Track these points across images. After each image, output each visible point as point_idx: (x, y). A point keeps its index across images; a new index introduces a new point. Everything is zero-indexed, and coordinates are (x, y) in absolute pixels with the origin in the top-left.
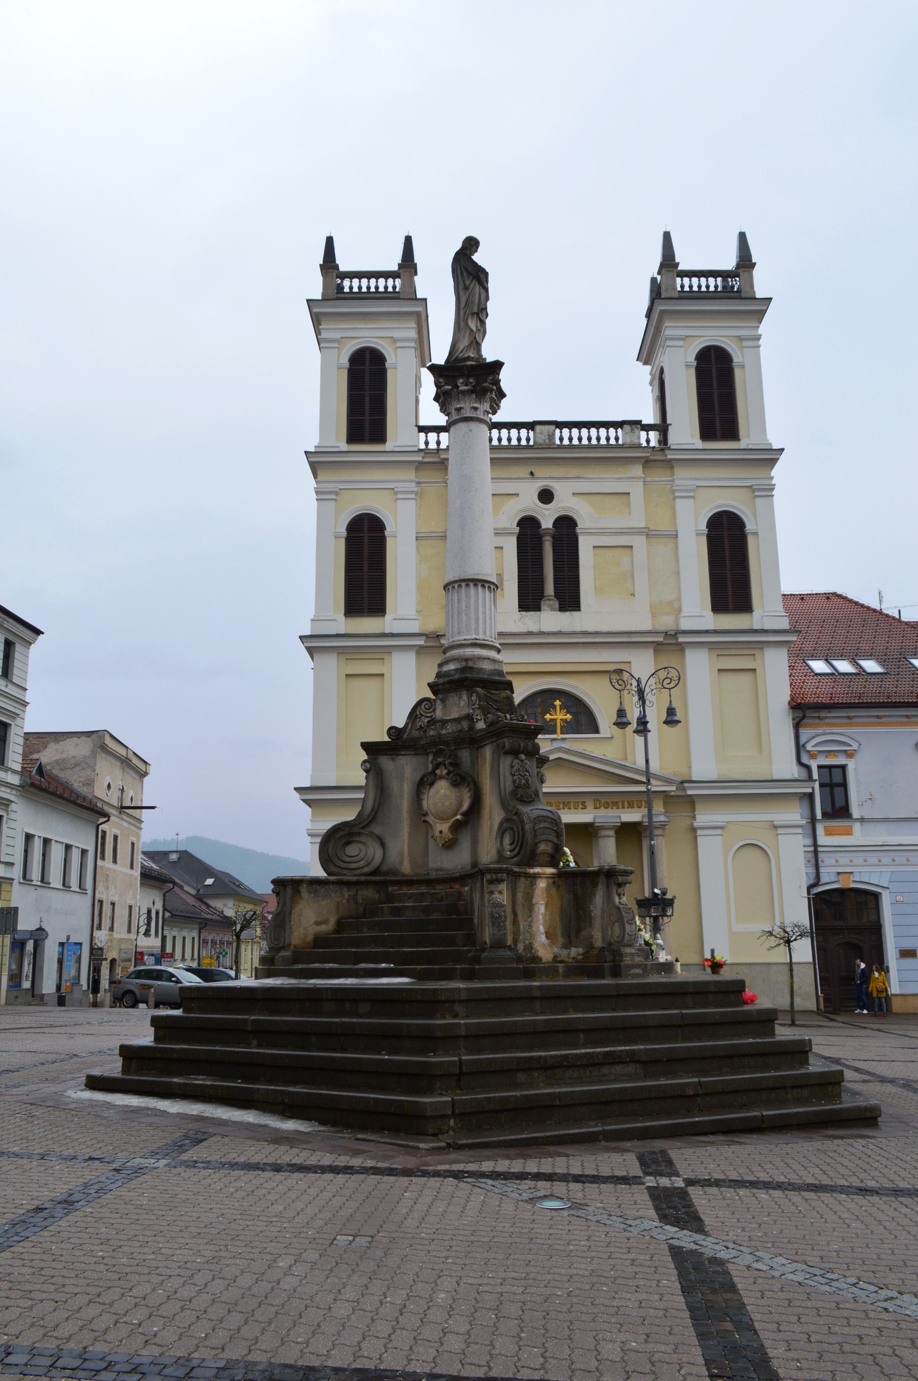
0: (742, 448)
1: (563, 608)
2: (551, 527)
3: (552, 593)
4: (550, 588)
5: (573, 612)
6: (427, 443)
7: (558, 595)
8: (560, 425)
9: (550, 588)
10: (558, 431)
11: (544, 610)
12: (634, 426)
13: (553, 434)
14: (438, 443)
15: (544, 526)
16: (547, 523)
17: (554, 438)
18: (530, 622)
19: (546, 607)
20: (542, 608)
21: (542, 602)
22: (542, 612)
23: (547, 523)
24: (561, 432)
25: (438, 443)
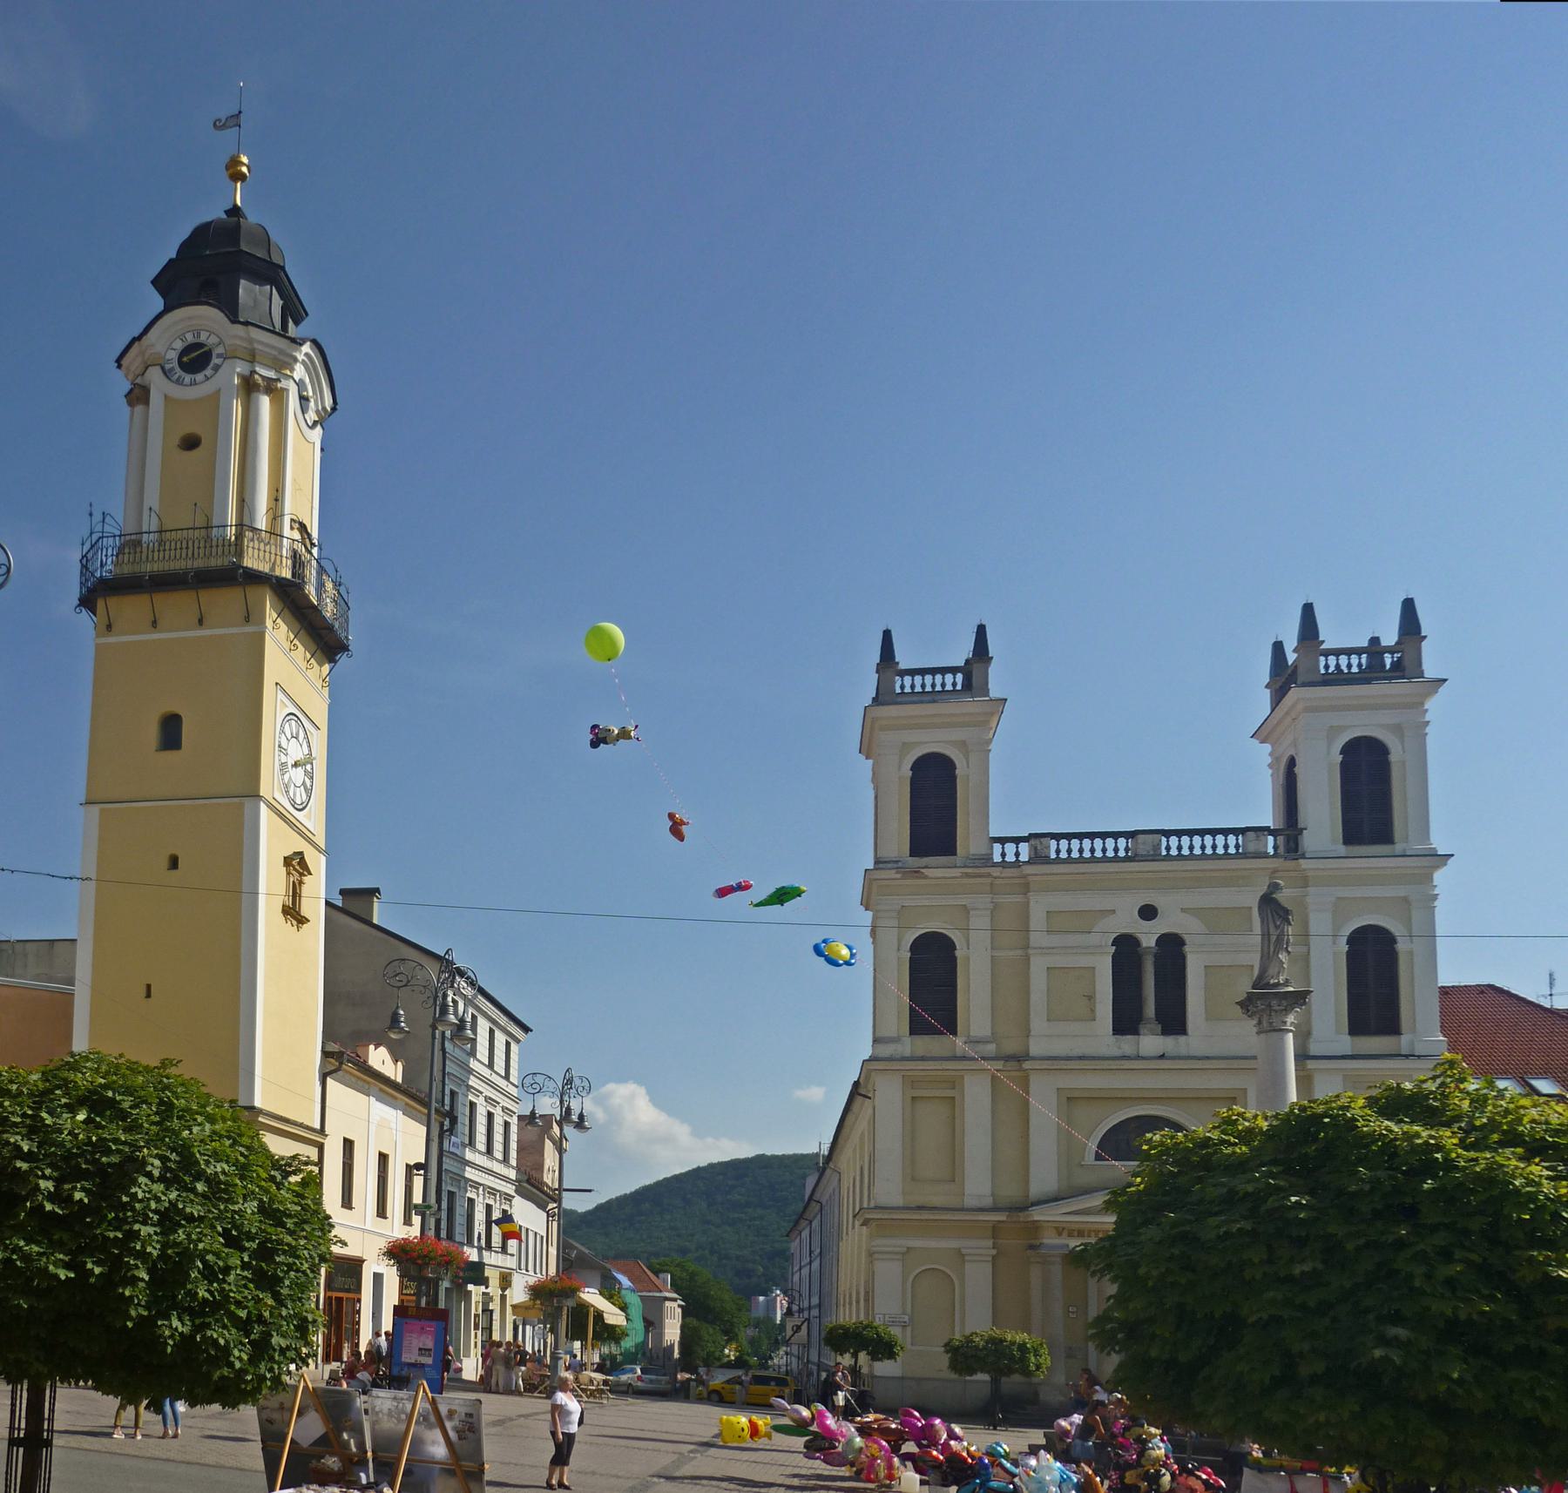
0: (1397, 853)
1: (1166, 1031)
2: (1153, 945)
3: (1153, 1016)
4: (1150, 1009)
5: (1178, 1037)
6: (1003, 855)
7: (1160, 1017)
8: (1167, 833)
9: (1150, 1009)
10: (1164, 839)
11: (1144, 1035)
12: (1258, 833)
13: (1159, 844)
14: (1017, 854)
15: (1144, 945)
16: (1149, 941)
17: (1160, 848)
18: (1127, 1044)
19: (1145, 1031)
20: (1142, 1032)
21: (1141, 1026)
22: (1141, 1037)
23: (1149, 941)
24: (1168, 841)
25: (1017, 854)
